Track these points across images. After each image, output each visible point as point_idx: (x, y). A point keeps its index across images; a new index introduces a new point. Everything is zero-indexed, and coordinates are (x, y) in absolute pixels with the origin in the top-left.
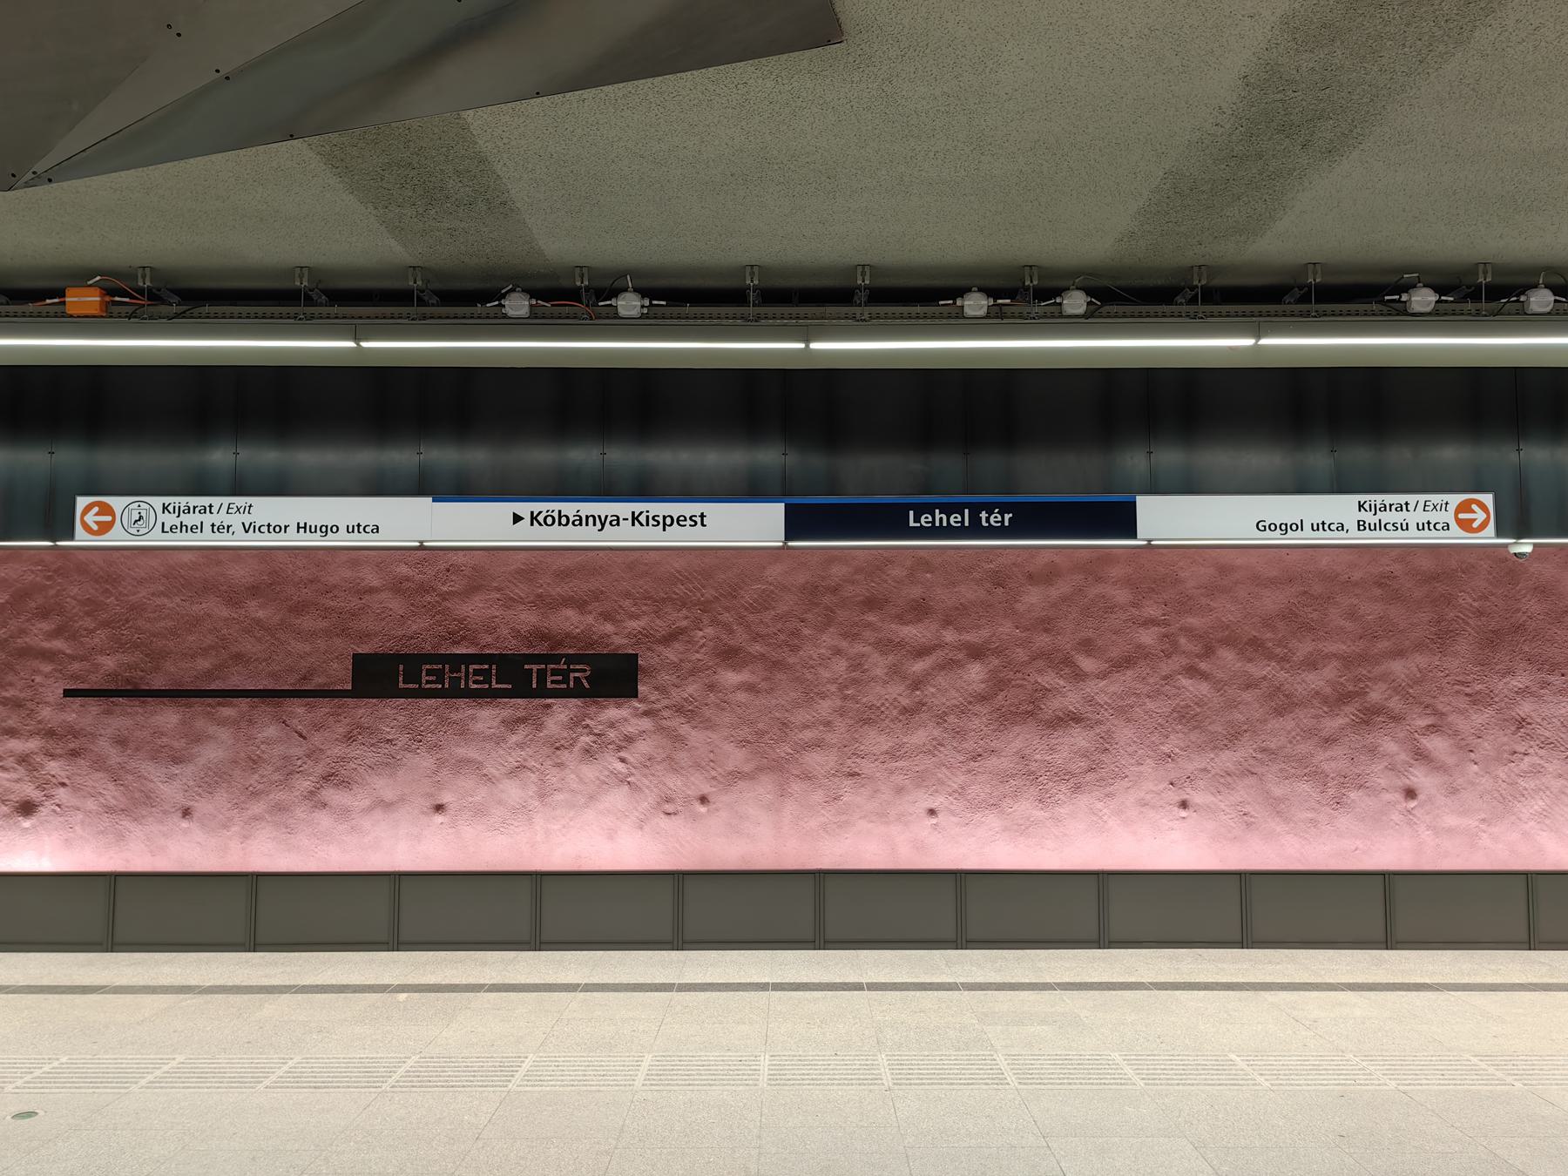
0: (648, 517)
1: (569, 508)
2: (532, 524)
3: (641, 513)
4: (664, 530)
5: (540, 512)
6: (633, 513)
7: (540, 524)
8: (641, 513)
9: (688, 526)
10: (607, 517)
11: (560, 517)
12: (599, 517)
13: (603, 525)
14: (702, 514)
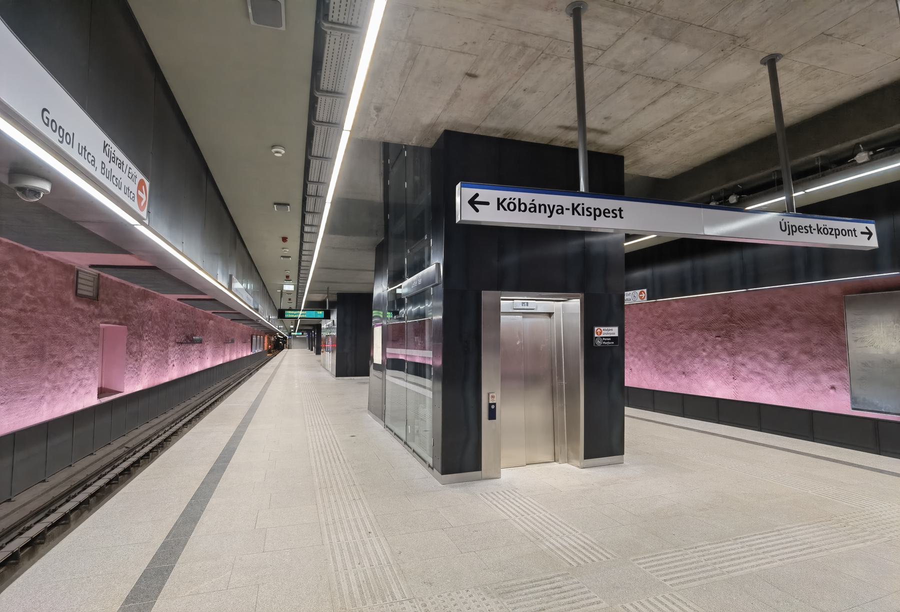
0: (583, 208)
1: (527, 197)
2: (499, 209)
3: (578, 205)
4: (595, 219)
5: (505, 200)
6: (573, 205)
7: (505, 210)
8: (578, 205)
9: (611, 217)
10: (554, 206)
11: (520, 205)
12: (549, 206)
13: (552, 213)
14: (620, 208)
